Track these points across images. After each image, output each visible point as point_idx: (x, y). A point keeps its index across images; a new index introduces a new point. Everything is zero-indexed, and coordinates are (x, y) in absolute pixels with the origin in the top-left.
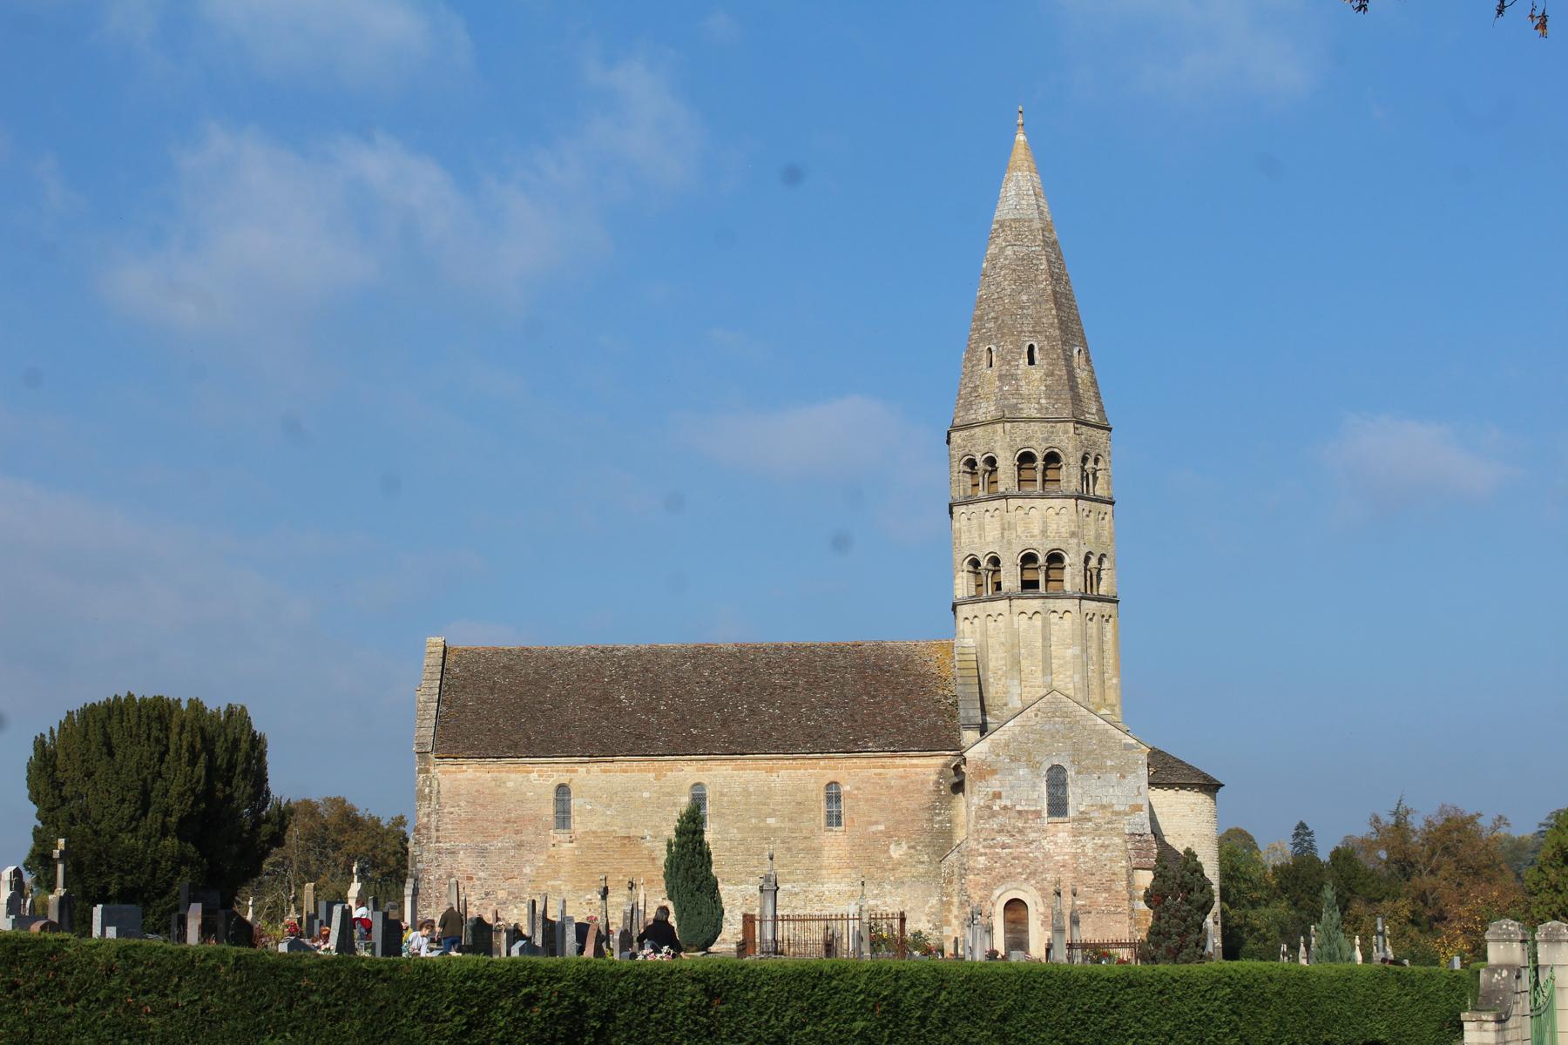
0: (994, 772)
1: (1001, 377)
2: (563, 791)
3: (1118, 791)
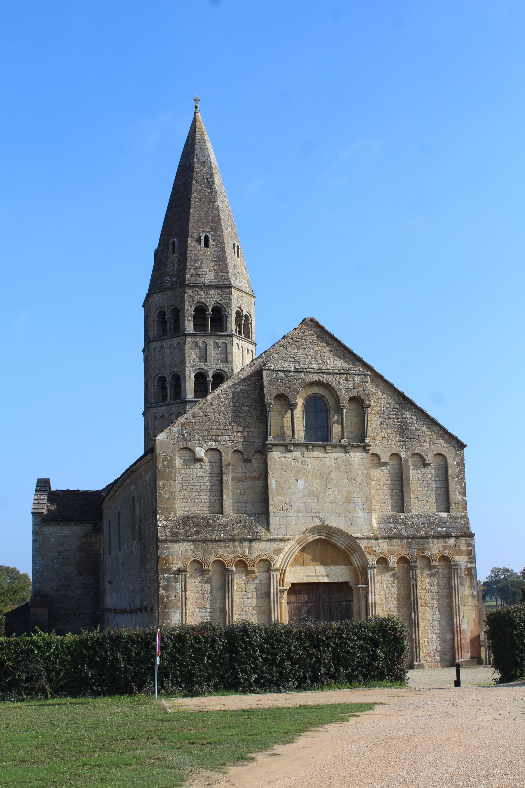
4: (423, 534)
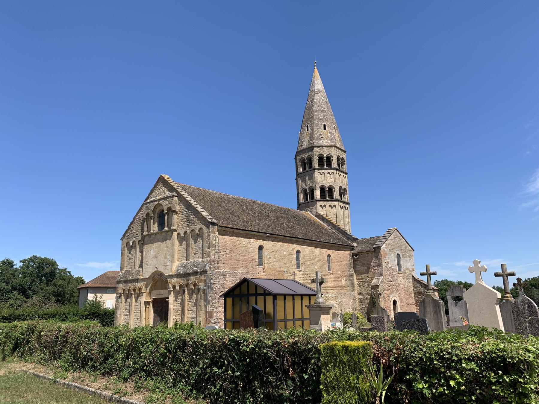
0: (387, 254)
1: (330, 133)
2: (261, 248)
3: (409, 264)
4: (188, 272)
